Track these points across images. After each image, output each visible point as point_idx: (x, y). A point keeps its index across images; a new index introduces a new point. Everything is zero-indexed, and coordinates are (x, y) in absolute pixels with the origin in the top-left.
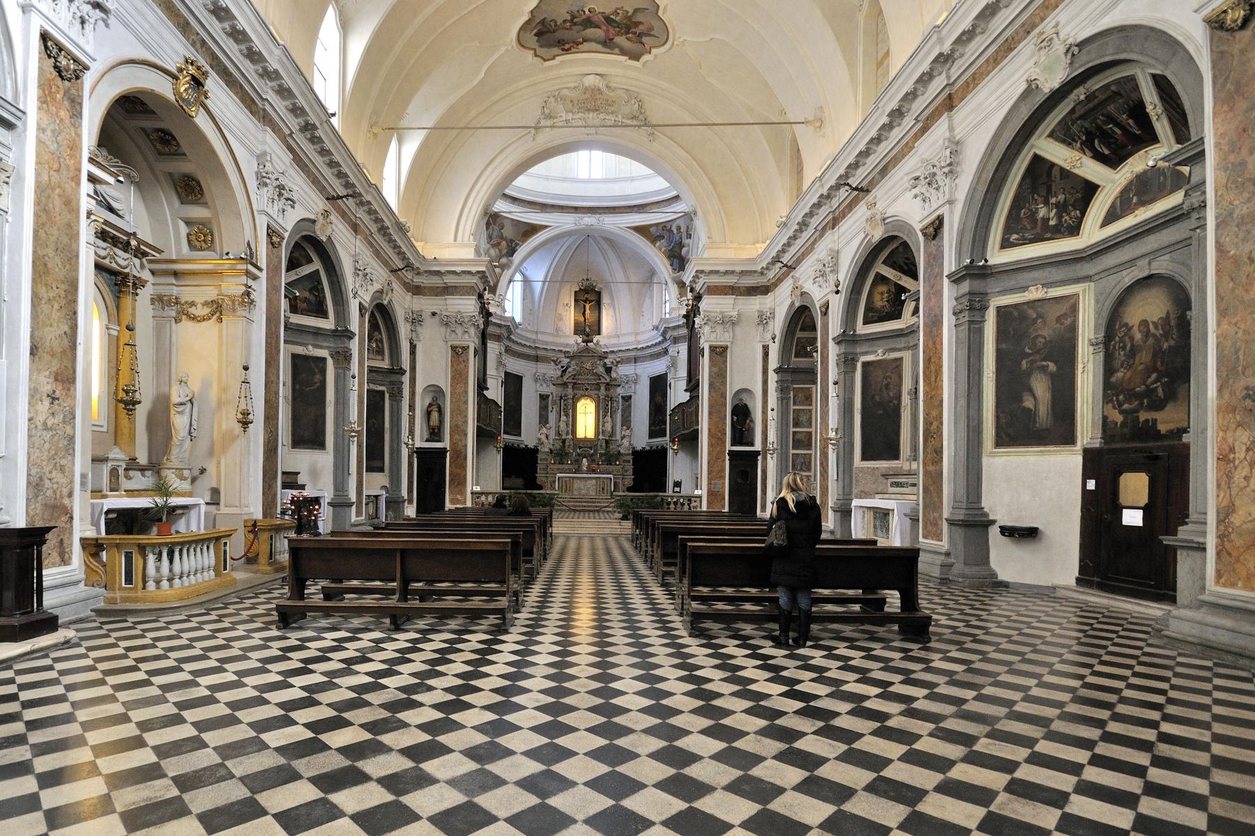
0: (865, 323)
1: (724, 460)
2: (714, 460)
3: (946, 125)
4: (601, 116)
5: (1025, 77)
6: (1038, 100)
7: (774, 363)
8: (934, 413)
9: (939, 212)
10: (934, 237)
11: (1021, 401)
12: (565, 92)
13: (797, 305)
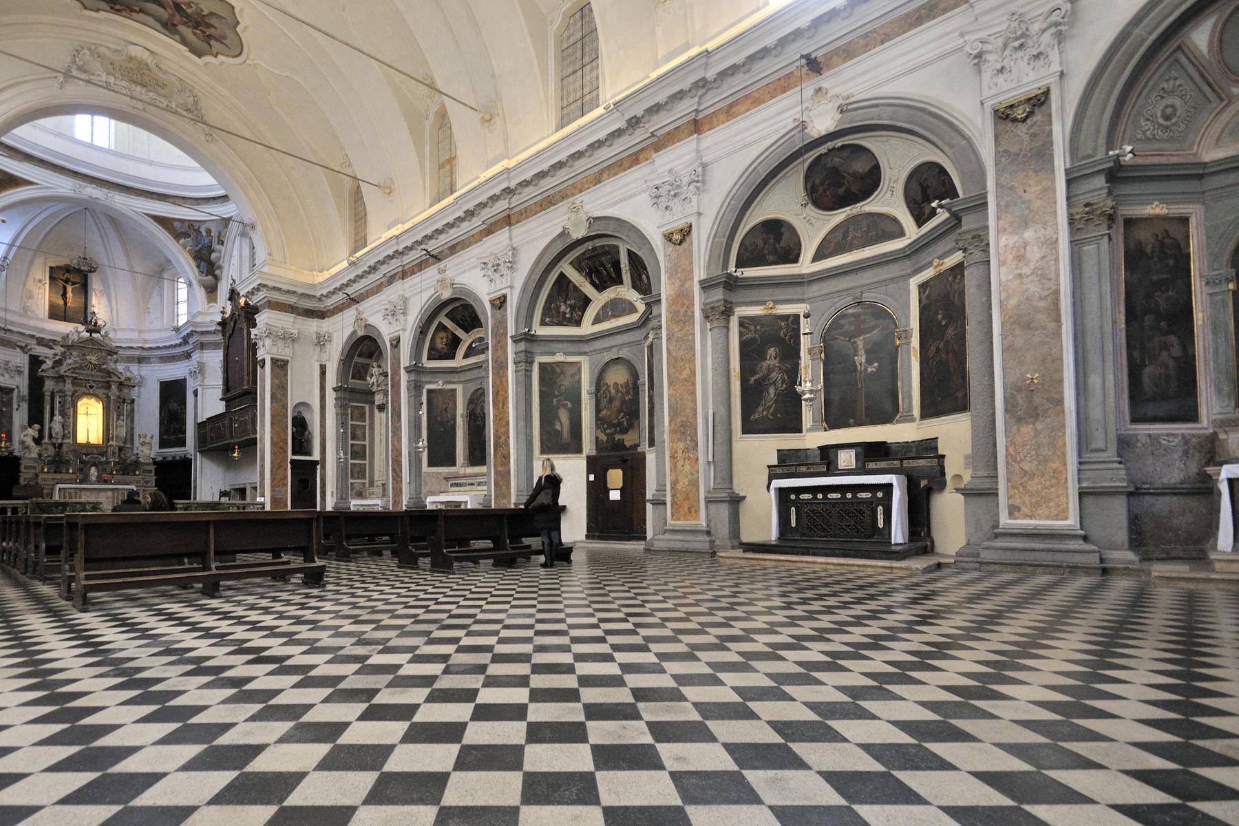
0: (428, 359)
1: (286, 469)
2: (277, 467)
3: (507, 235)
4: (151, 94)
5: (562, 224)
6: (569, 242)
7: (332, 380)
8: (502, 430)
9: (504, 292)
10: (500, 308)
11: (554, 424)
12: (103, 50)
13: (360, 333)
